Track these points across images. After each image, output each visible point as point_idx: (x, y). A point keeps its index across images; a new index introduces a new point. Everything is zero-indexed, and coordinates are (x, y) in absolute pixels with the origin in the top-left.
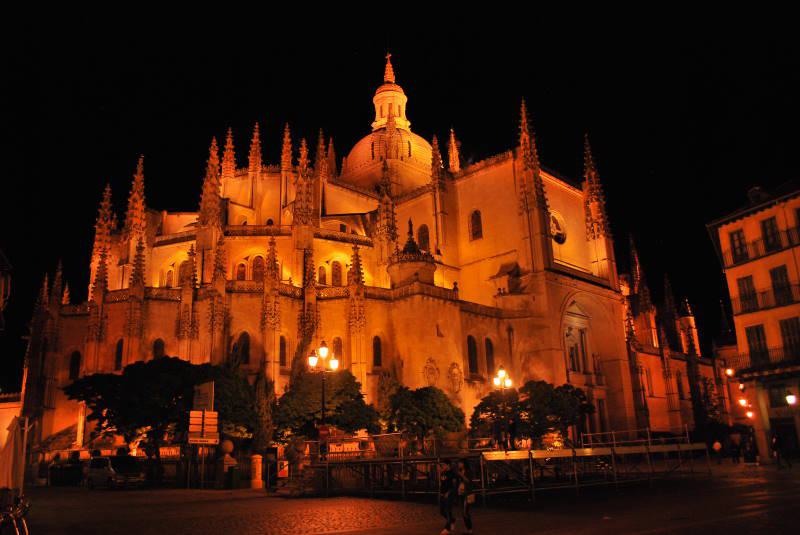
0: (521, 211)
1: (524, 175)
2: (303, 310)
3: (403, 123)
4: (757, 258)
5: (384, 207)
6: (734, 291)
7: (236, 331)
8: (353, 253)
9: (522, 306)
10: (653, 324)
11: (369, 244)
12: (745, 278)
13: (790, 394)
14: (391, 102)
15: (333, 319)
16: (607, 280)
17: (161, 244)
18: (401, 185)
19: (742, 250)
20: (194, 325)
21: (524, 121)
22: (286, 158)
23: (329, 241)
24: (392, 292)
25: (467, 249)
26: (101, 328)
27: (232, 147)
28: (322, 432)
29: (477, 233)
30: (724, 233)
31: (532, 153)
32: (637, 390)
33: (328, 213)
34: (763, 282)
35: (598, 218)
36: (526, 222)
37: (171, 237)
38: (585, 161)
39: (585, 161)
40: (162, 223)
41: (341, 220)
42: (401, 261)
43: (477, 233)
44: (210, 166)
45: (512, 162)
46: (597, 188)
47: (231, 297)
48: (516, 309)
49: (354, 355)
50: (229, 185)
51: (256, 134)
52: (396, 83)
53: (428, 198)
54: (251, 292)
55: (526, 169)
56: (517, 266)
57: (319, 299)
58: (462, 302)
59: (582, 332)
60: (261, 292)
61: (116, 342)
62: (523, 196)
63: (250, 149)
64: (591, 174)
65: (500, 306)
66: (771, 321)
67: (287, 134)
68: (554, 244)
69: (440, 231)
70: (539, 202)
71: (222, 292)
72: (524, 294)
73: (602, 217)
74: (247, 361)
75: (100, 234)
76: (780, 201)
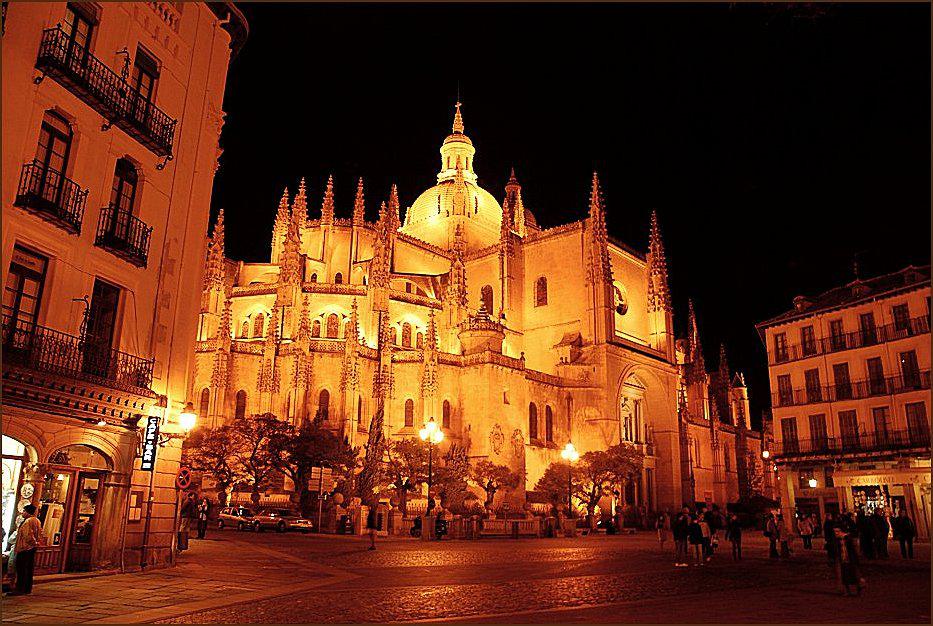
2: (379, 372)
3: (470, 176)
4: (796, 360)
5: (455, 271)
6: (774, 387)
7: (319, 386)
8: (429, 319)
10: (706, 395)
13: (812, 477)
14: (457, 153)
15: (406, 383)
17: (243, 294)
19: (783, 352)
21: (595, 192)
22: (359, 211)
23: (403, 303)
24: (463, 358)
25: (531, 314)
29: (542, 300)
30: (770, 333)
31: (601, 227)
32: (685, 461)
33: (396, 271)
34: (798, 382)
43: (542, 300)
50: (311, 240)
52: (466, 133)
53: (495, 259)
54: (332, 352)
55: (594, 242)
56: (580, 337)
57: (393, 361)
58: (530, 372)
59: (636, 402)
61: (201, 390)
62: (589, 268)
64: (655, 245)
65: (561, 375)
66: (802, 414)
69: (506, 295)
74: (326, 418)
76: (817, 314)
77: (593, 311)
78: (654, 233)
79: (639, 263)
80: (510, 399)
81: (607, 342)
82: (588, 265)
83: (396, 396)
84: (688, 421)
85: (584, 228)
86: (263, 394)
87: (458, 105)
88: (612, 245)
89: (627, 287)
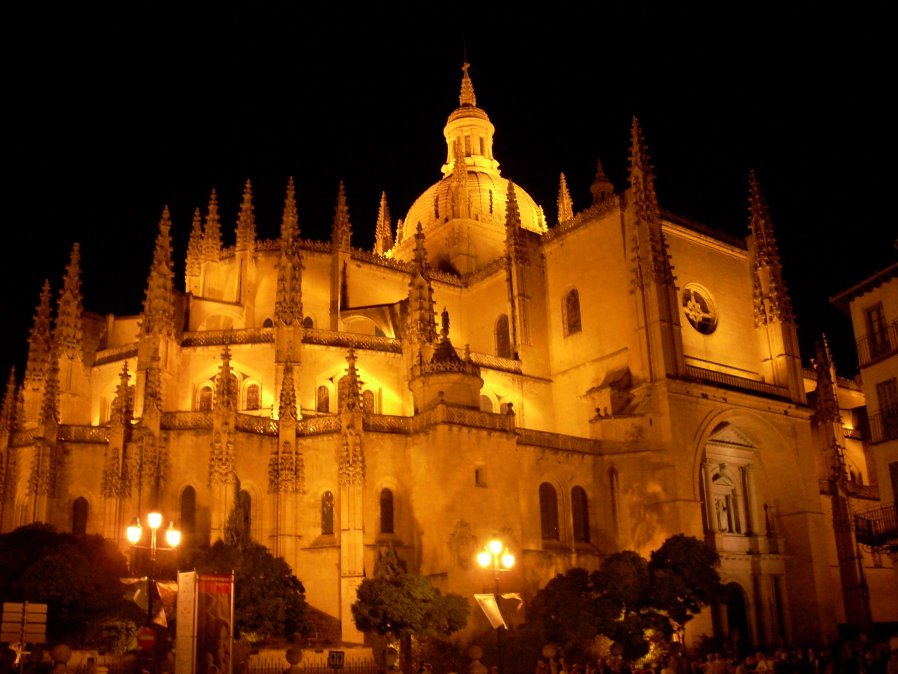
0: (631, 287)
1: (636, 233)
2: (277, 453)
3: (489, 165)
9: (632, 435)
11: (396, 349)
12: (885, 383)
16: (786, 387)
18: (476, 257)
20: (124, 477)
21: (635, 149)
23: (333, 348)
26: (6, 483)
27: (217, 217)
28: (297, 634)
29: (574, 326)
31: (647, 198)
35: (771, 291)
36: (640, 305)
37: (116, 352)
38: (749, 204)
39: (749, 204)
40: (107, 332)
41: (365, 314)
42: (425, 375)
43: (574, 326)
44: (158, 248)
45: (618, 212)
46: (769, 244)
47: (168, 435)
48: (623, 440)
49: (344, 517)
51: (247, 197)
52: (477, 106)
56: (628, 372)
57: (300, 435)
60: (208, 429)
62: (635, 265)
63: (238, 218)
64: (758, 223)
65: (599, 438)
67: (291, 193)
68: (691, 337)
70: (658, 271)
71: (155, 428)
72: (635, 416)
73: (776, 289)
75: (35, 350)
77: (643, 331)
78: (755, 204)
79: (737, 254)
80: (489, 477)
81: (668, 376)
82: (633, 260)
83: (305, 489)
84: (849, 494)
85: (623, 206)
86: (108, 500)
87: (466, 66)
88: (670, 224)
89: (714, 290)
